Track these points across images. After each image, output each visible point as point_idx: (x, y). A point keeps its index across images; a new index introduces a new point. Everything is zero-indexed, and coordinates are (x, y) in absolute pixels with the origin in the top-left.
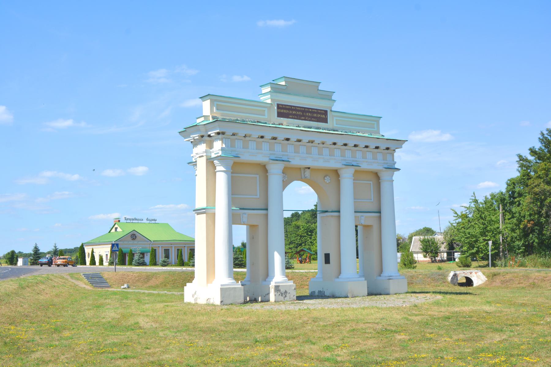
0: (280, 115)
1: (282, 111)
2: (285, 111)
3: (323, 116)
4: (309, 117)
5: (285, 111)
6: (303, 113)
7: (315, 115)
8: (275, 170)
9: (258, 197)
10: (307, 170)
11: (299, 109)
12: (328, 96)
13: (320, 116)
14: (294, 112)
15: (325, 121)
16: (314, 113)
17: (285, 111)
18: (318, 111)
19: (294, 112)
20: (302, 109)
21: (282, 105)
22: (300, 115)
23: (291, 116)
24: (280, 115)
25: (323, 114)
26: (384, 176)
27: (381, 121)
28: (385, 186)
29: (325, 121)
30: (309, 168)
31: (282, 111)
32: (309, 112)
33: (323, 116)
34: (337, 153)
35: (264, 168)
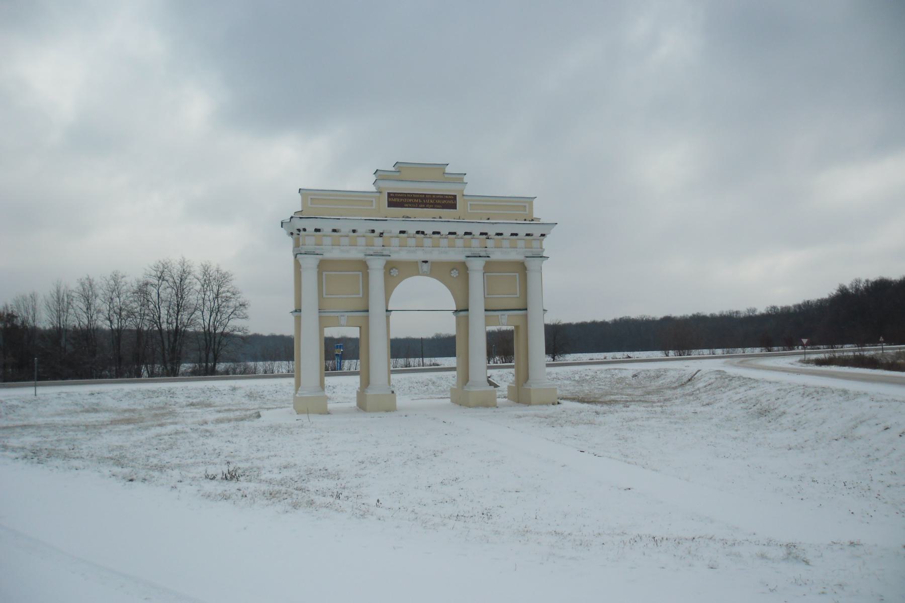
0: (391, 204)
2: (397, 200)
4: (430, 204)
7: (439, 201)
8: (377, 266)
9: (361, 296)
12: (459, 178)
13: (448, 202)
15: (454, 206)
18: (443, 197)
22: (419, 204)
24: (391, 204)
25: (450, 199)
26: (532, 264)
27: (535, 201)
28: (532, 277)
29: (454, 206)
30: (426, 262)
31: (394, 200)
32: (430, 199)
33: (451, 202)
34: (459, 242)
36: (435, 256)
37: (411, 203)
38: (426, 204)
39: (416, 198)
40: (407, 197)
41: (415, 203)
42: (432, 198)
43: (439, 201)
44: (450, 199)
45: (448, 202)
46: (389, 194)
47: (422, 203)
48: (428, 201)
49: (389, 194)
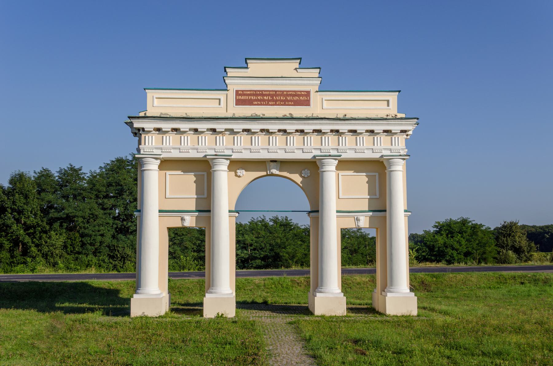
1: (243, 98)
3: (305, 98)
10: (272, 163)
14: (259, 98)
15: (307, 103)
16: (291, 95)
18: (295, 94)
19: (259, 98)
20: (272, 93)
21: (243, 91)
22: (269, 101)
24: (239, 102)
25: (302, 95)
29: (307, 103)
31: (243, 98)
32: (281, 95)
33: (305, 98)
36: (281, 155)
37: (260, 100)
38: (276, 101)
39: (266, 95)
40: (256, 95)
41: (264, 100)
42: (284, 96)
44: (302, 95)
47: (273, 100)
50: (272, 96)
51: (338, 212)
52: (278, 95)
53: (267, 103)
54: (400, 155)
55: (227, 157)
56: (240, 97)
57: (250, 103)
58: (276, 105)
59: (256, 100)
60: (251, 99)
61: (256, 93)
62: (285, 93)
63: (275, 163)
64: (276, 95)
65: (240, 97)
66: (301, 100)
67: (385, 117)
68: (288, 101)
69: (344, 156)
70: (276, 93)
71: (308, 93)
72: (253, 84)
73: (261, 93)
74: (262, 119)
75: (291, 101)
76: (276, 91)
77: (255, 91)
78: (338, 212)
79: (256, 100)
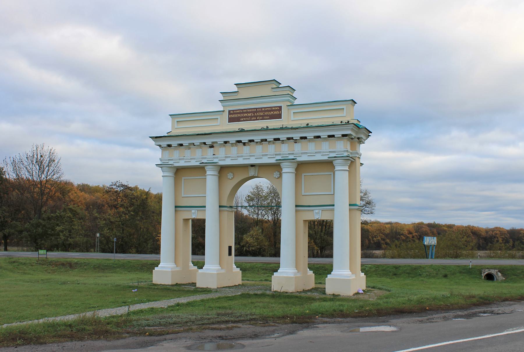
0: (231, 120)
4: (260, 116)
5: (236, 116)
6: (254, 114)
7: (267, 113)
11: (251, 111)
15: (279, 116)
17: (236, 116)
18: (271, 109)
20: (253, 110)
21: (233, 111)
22: (251, 117)
23: (242, 119)
24: (231, 120)
29: (279, 116)
32: (260, 112)
33: (277, 112)
35: (200, 169)
38: (257, 116)
39: (249, 112)
41: (248, 117)
42: (262, 111)
43: (267, 113)
45: (275, 113)
46: (229, 111)
47: (254, 116)
48: (258, 114)
49: (229, 111)
50: (254, 112)
51: (205, 207)
52: (258, 112)
53: (250, 119)
54: (342, 157)
55: (214, 164)
56: (232, 116)
57: (238, 120)
58: (257, 120)
59: (242, 117)
60: (239, 117)
61: (242, 111)
62: (263, 109)
63: (253, 167)
64: (256, 112)
65: (232, 116)
66: (275, 114)
67: (340, 123)
68: (265, 116)
69: (299, 159)
70: (256, 110)
71: (280, 107)
72: (232, 106)
73: (246, 111)
74: (297, 128)
75: (267, 115)
76: (256, 109)
77: (242, 110)
78: (350, 205)
79: (242, 117)
